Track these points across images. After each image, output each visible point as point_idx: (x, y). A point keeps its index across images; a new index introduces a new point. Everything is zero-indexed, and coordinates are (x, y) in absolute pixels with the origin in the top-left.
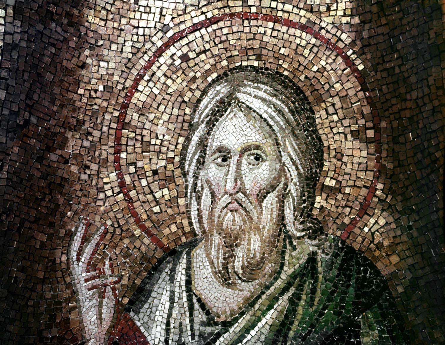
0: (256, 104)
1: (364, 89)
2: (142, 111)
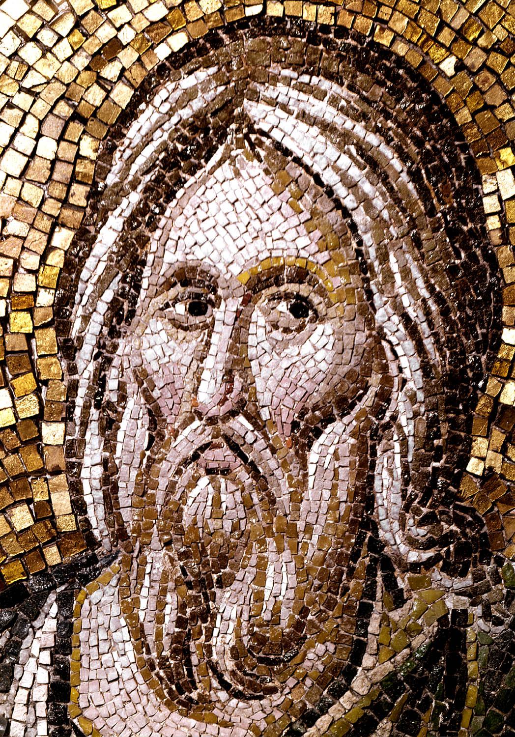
0: (302, 140)
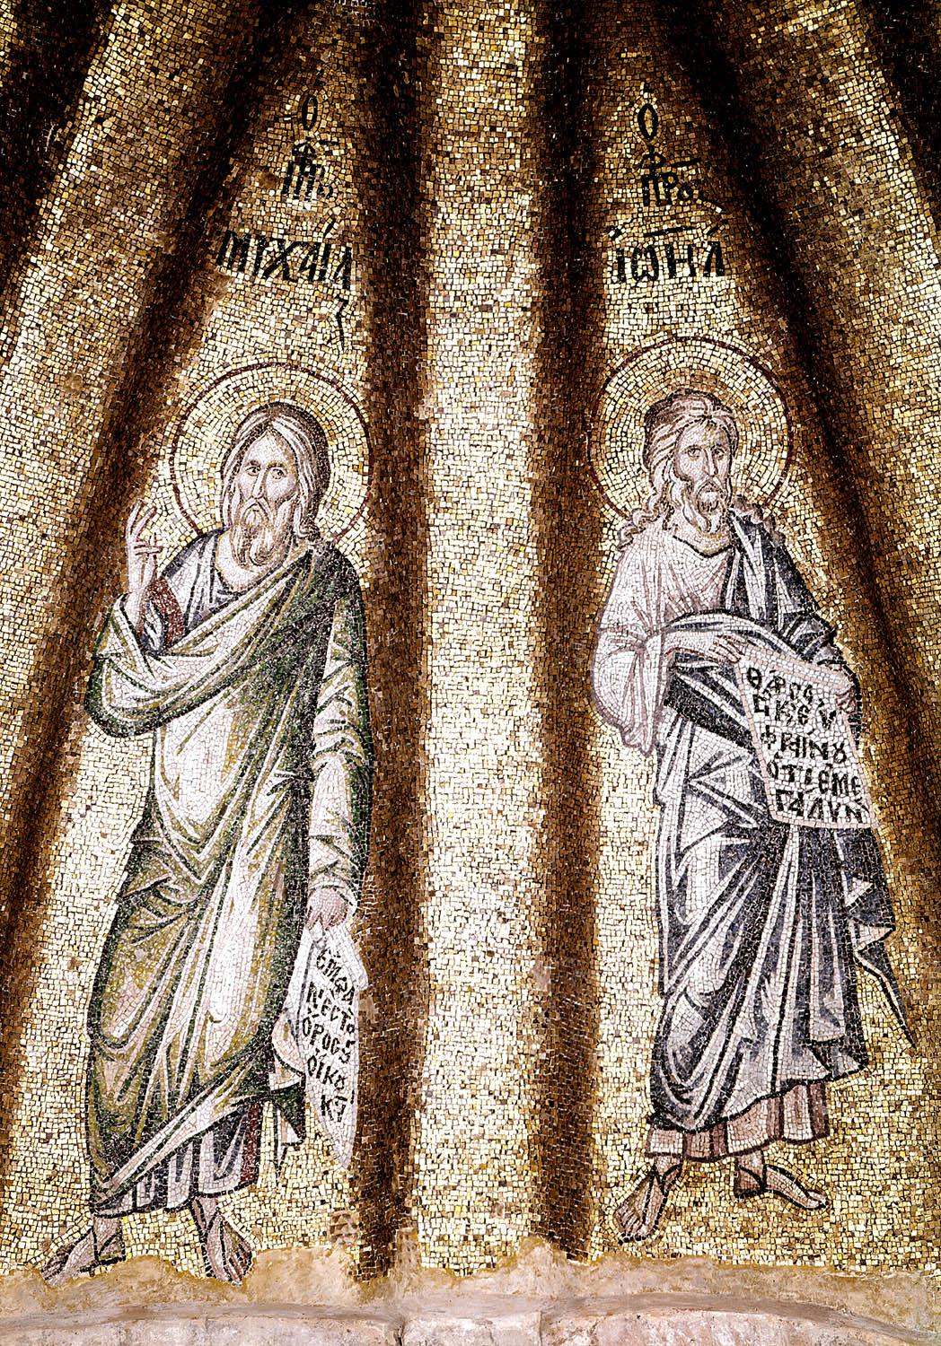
0: (285, 432)
1: (367, 436)
2: (198, 424)
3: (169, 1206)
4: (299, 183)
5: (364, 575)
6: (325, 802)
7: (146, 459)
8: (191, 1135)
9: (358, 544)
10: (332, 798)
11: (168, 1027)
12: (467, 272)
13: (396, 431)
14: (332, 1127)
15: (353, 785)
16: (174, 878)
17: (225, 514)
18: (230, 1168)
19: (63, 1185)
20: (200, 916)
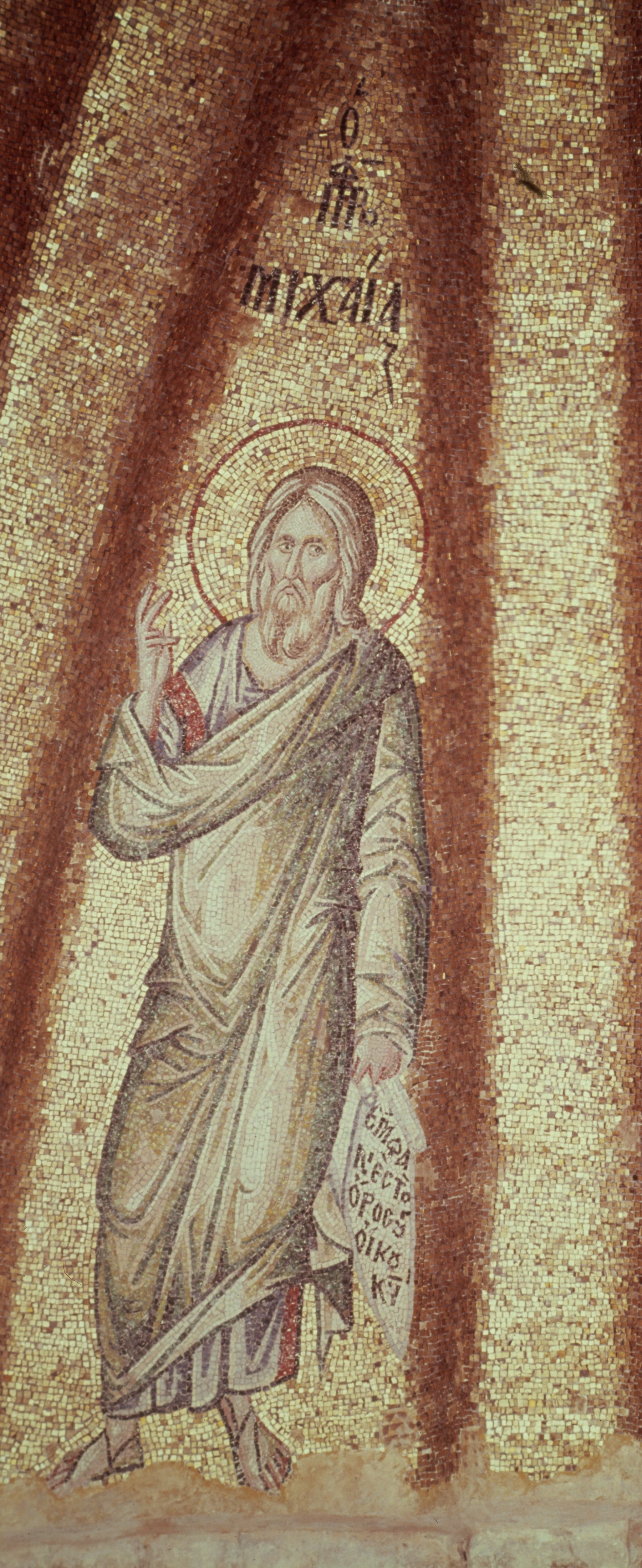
1: (421, 504)
2: (221, 493)
3: (194, 1405)
4: (338, 208)
5: (419, 669)
6: (374, 935)
7: (159, 535)
8: (218, 1323)
9: (409, 632)
10: (382, 932)
11: (191, 1198)
12: (541, 312)
13: (455, 499)
14: (384, 1310)
15: (408, 914)
16: (196, 1026)
17: (253, 597)
18: (265, 1360)
19: (70, 1381)
20: (228, 1070)
